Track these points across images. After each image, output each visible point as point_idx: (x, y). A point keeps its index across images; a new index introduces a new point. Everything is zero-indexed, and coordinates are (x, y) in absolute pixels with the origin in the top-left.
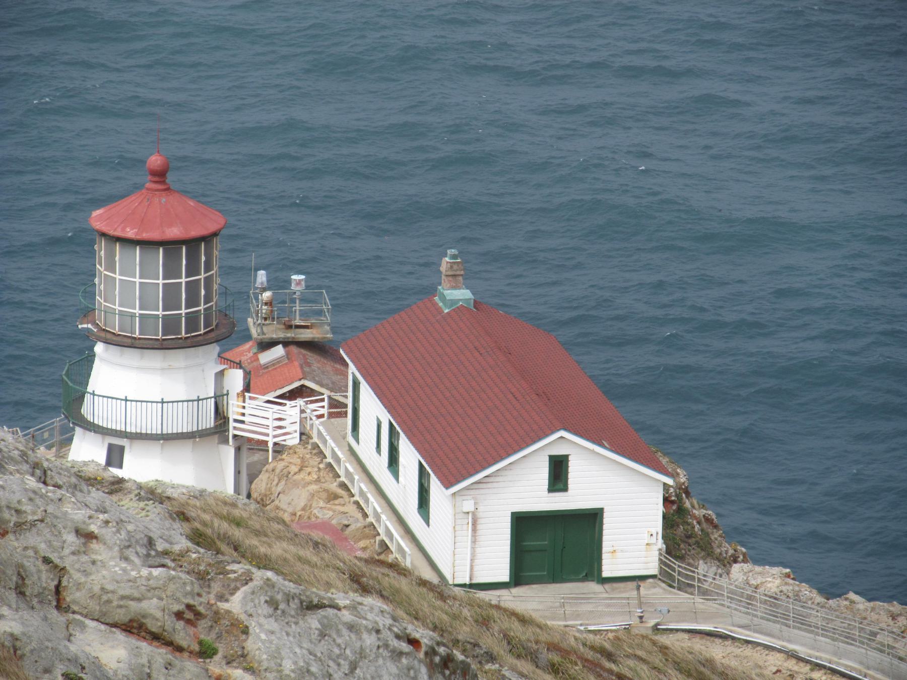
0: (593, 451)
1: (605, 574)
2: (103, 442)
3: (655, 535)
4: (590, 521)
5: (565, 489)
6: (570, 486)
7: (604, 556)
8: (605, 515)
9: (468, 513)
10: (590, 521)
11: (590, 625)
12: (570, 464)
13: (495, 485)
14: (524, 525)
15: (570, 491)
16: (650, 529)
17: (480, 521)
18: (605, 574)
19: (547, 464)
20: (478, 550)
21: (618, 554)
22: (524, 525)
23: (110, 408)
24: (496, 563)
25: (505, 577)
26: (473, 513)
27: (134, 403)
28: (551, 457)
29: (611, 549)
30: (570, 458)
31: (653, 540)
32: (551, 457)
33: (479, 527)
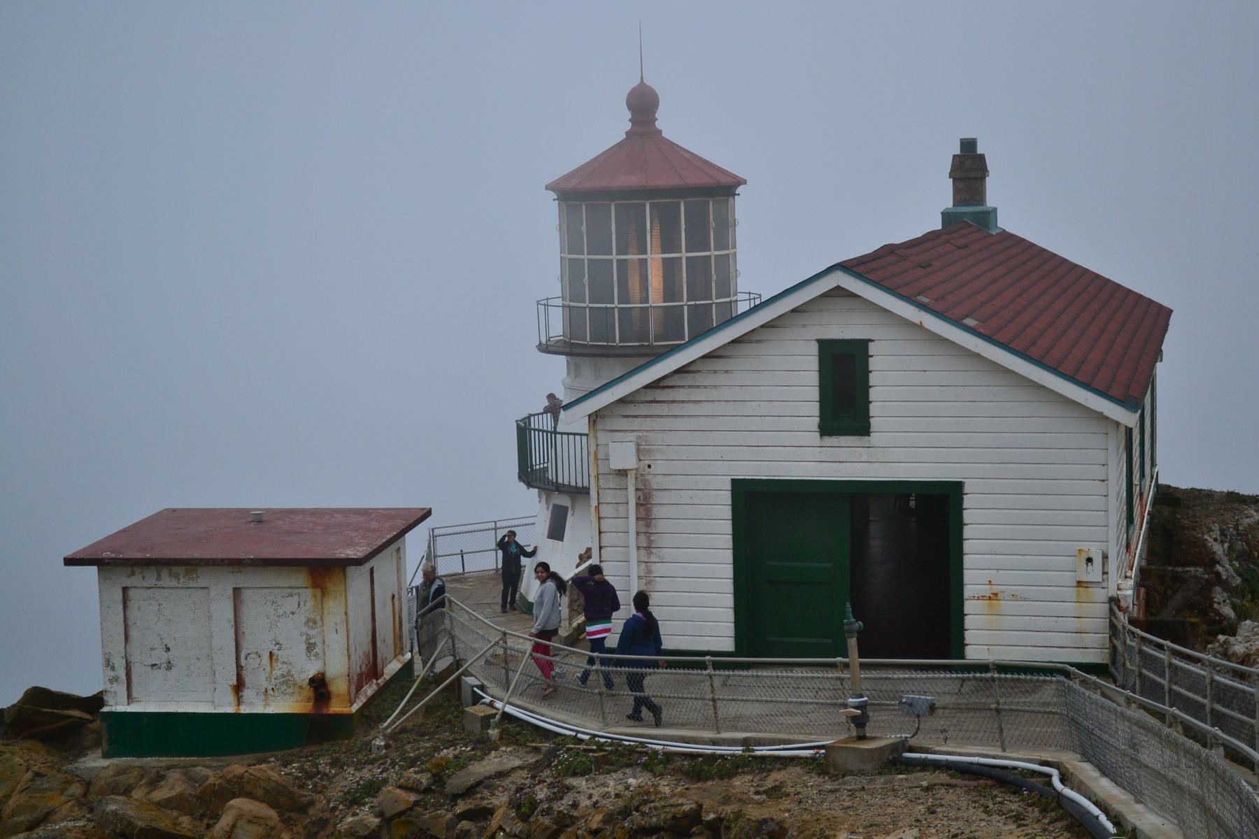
0: (920, 327)
1: (975, 652)
2: (547, 502)
3: (1098, 560)
4: (929, 518)
5: (861, 427)
6: (875, 423)
7: (969, 606)
8: (967, 501)
9: (623, 473)
10: (929, 518)
11: (760, 742)
12: (873, 364)
13: (691, 409)
14: (761, 508)
15: (875, 438)
16: (1084, 546)
17: (658, 498)
18: (975, 652)
19: (813, 363)
20: (658, 569)
21: (1006, 605)
22: (761, 508)
23: (566, 460)
24: (698, 602)
25: (728, 645)
26: (640, 477)
27: (565, 437)
28: (824, 345)
29: (987, 590)
30: (872, 348)
31: (1094, 573)
32: (824, 345)
33: (657, 512)
